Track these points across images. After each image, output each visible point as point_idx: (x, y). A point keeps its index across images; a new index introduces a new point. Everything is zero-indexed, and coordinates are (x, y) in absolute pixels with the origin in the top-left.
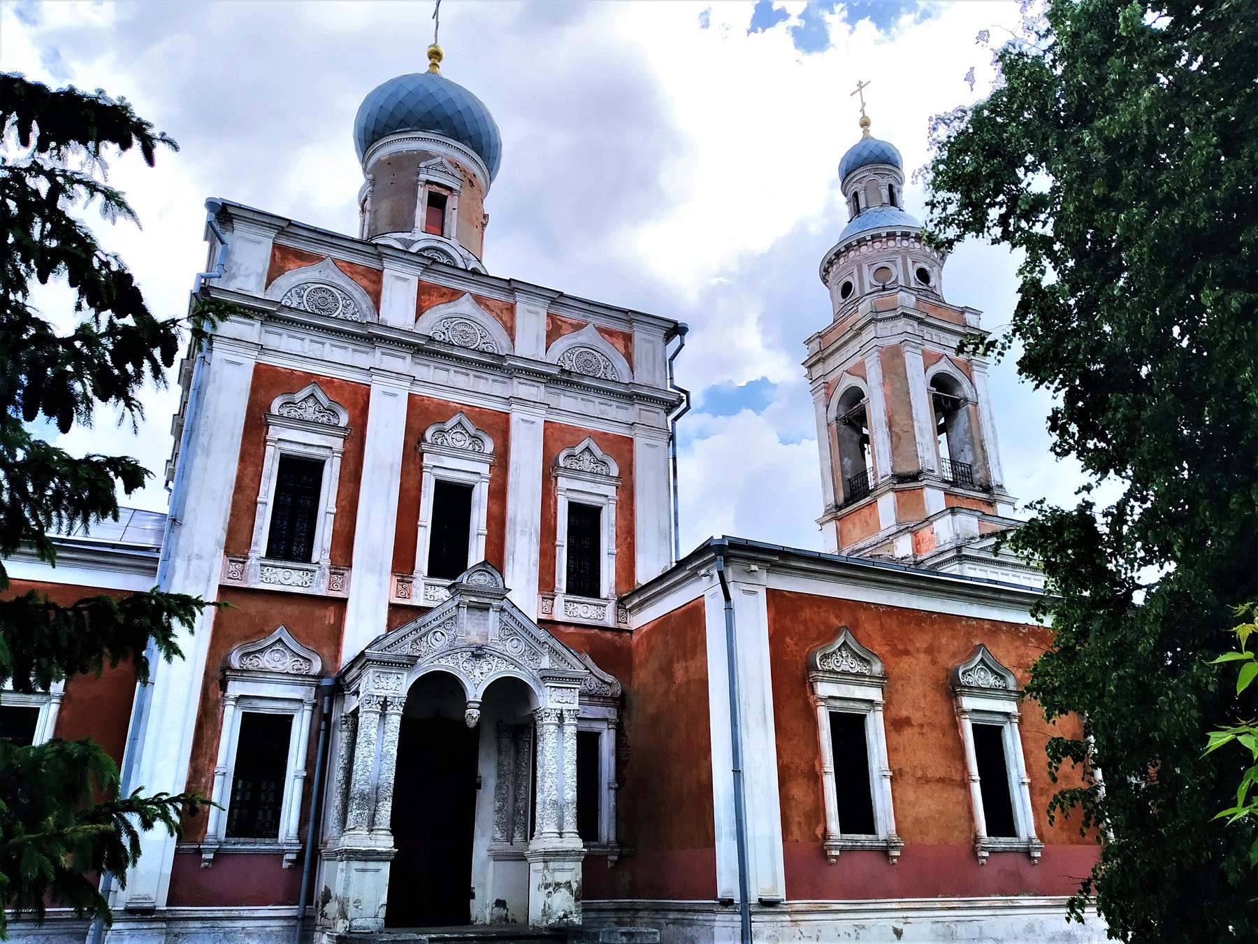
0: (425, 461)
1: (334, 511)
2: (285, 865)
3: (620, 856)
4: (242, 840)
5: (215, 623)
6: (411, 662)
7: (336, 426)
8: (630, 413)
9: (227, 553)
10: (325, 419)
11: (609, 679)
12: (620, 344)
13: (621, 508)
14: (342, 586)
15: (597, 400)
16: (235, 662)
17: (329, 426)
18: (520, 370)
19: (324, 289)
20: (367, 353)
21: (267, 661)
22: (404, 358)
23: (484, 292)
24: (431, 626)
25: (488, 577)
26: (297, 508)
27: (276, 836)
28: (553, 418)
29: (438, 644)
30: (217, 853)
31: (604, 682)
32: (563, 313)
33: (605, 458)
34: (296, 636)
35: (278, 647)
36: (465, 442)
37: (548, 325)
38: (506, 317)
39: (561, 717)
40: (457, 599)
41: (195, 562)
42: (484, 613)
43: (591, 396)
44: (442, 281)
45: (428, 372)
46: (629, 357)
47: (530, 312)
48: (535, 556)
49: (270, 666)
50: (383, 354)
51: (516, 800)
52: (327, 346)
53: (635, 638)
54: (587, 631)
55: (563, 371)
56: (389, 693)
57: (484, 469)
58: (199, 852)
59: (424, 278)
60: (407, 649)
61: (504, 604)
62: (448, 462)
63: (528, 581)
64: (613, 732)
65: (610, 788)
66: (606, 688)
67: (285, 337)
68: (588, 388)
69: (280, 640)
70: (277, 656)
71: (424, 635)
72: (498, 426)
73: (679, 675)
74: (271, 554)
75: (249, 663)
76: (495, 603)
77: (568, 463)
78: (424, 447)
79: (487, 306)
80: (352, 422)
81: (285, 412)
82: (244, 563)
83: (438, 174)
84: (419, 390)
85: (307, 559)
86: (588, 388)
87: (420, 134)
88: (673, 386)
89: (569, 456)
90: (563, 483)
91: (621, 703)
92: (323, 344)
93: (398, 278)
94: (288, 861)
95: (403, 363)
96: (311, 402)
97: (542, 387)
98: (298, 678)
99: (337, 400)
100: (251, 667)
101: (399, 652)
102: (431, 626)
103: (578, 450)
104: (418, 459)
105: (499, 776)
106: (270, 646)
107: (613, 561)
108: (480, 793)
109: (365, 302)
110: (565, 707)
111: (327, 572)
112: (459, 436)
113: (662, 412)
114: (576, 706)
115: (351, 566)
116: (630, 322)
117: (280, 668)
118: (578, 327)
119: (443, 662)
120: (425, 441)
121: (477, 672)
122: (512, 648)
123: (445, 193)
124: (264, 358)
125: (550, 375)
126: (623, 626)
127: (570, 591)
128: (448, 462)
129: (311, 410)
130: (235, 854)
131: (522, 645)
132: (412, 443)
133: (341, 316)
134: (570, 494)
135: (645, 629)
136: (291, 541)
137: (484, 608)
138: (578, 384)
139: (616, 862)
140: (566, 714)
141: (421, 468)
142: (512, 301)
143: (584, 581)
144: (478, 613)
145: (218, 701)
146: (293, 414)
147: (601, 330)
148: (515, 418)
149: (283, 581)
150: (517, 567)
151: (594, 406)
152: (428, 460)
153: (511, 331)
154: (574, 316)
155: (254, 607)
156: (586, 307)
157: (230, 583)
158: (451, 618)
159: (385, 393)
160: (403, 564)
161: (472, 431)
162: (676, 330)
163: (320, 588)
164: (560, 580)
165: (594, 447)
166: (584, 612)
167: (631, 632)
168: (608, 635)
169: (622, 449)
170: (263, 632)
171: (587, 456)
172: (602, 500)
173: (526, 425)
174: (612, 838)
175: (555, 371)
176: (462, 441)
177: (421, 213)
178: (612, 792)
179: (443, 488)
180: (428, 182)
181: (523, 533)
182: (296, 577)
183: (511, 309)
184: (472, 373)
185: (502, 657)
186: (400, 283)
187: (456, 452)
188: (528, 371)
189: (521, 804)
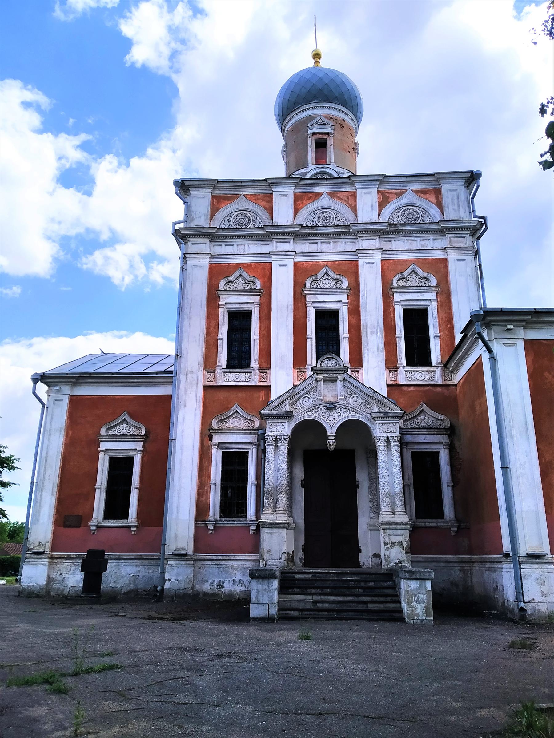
1: (258, 337)
2: (251, 532)
3: (459, 528)
4: (228, 519)
5: (203, 406)
6: (289, 416)
7: (255, 290)
8: (443, 242)
9: (205, 369)
10: (249, 287)
11: (441, 417)
12: (433, 198)
13: (442, 306)
15: (418, 239)
16: (215, 425)
17: (251, 290)
18: (361, 231)
19: (242, 213)
20: (268, 244)
21: (231, 423)
22: (289, 242)
23: (335, 189)
24: (301, 394)
25: (334, 361)
26: (240, 339)
27: (246, 517)
29: (307, 404)
30: (215, 525)
32: (389, 188)
33: (426, 275)
34: (245, 409)
35: (236, 415)
37: (379, 198)
38: (351, 201)
39: (388, 441)
41: (190, 376)
42: (335, 383)
43: (414, 236)
44: (308, 190)
45: (303, 247)
46: (439, 205)
47: (365, 193)
48: (382, 346)
49: (233, 426)
50: (277, 242)
52: (246, 246)
54: (423, 388)
55: (390, 225)
56: (278, 434)
57: (344, 298)
58: (206, 525)
59: (297, 191)
60: (288, 408)
61: (345, 376)
63: (379, 362)
64: (447, 451)
65: (448, 486)
66: (440, 423)
67: (223, 246)
68: (410, 232)
69: (236, 411)
70: (236, 420)
72: (351, 270)
75: (222, 425)
77: (400, 284)
78: (306, 292)
79: (338, 197)
80: (263, 286)
81: (227, 288)
82: (214, 372)
83: (318, 127)
84: (300, 259)
85: (248, 366)
86: (410, 232)
87: (306, 106)
88: (475, 216)
89: (400, 279)
91: (451, 431)
92: (244, 245)
93: (281, 195)
95: (289, 245)
97: (378, 239)
98: (248, 431)
99: (254, 275)
100: (223, 427)
101: (282, 410)
103: (406, 274)
104: (303, 298)
105: (370, 480)
107: (438, 341)
108: (359, 490)
109: (264, 215)
110: (390, 435)
111: (258, 371)
112: (327, 281)
113: (467, 236)
116: (438, 181)
117: (239, 427)
118: (400, 194)
119: (310, 414)
120: (305, 288)
121: (331, 418)
123: (324, 137)
124: (214, 260)
125: (382, 229)
127: (409, 364)
129: (241, 284)
130: (224, 526)
132: (299, 291)
133: (253, 226)
134: (403, 303)
135: (461, 381)
136: (238, 358)
137: (334, 380)
138: (403, 231)
139: (457, 532)
141: (306, 304)
142: (354, 189)
143: (418, 356)
145: (209, 446)
146: (232, 288)
147: (417, 192)
149: (235, 379)
151: (417, 243)
152: (309, 299)
153: (354, 209)
154: (397, 188)
155: (222, 395)
156: (404, 179)
158: (313, 388)
159: (280, 265)
161: (334, 276)
162: (472, 178)
163: (255, 381)
164: (401, 359)
165: (417, 270)
166: (420, 376)
167: (455, 385)
168: (439, 389)
169: (440, 267)
170: (228, 409)
171: (413, 276)
172: (427, 303)
173: (369, 265)
174: (452, 516)
175: (384, 227)
176: (328, 284)
177: (311, 154)
178: (450, 488)
180: (314, 134)
181: (372, 333)
182: (242, 377)
183: (354, 195)
184: (332, 241)
185: (347, 408)
186: (283, 198)
187: (325, 291)
188: (367, 231)
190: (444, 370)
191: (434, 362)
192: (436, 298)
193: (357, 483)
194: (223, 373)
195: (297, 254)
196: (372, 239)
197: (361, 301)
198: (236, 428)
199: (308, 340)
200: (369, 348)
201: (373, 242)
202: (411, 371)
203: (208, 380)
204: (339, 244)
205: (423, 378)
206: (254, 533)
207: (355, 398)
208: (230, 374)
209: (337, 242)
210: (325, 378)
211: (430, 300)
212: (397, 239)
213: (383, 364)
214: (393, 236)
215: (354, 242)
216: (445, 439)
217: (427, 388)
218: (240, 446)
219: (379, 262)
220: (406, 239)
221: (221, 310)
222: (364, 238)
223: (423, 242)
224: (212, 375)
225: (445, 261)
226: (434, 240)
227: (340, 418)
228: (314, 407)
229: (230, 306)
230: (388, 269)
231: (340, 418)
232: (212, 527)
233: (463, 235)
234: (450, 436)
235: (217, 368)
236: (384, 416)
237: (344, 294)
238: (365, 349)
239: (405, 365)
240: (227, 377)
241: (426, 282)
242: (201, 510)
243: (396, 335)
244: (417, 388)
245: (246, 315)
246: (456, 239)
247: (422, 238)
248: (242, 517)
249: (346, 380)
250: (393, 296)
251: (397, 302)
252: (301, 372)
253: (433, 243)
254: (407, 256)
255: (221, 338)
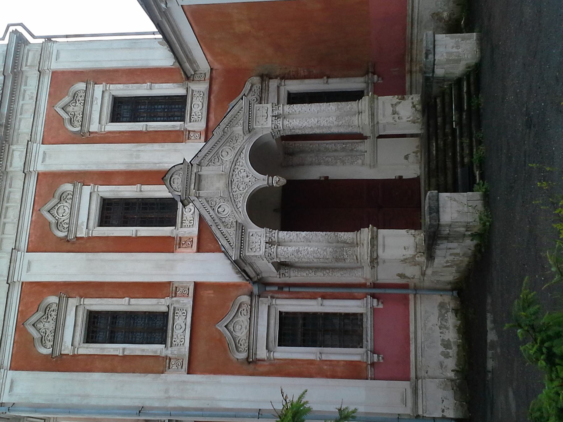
0: (83, 235)
1: (127, 299)
2: (381, 306)
3: (374, 73)
4: (364, 336)
5: (214, 374)
6: (241, 229)
7: (58, 305)
10: (54, 314)
11: (248, 86)
14: (185, 287)
15: (21, 102)
16: (242, 356)
21: (241, 333)
25: (175, 176)
27: (362, 314)
28: (39, 137)
30: (374, 352)
31: (251, 90)
33: (71, 94)
36: (65, 207)
39: (277, 117)
40: (192, 198)
41: (171, 393)
42: (203, 178)
49: (245, 331)
51: (336, 151)
53: (217, 66)
57: (87, 190)
58: (373, 364)
60: (231, 232)
62: (83, 217)
63: (175, 150)
64: (288, 82)
66: (255, 88)
71: (220, 219)
72: (50, 182)
73: (244, 27)
74: (163, 341)
76: (195, 170)
77: (78, 124)
78: (72, 237)
80: (54, 294)
81: (49, 344)
85: (165, 315)
90: (94, 127)
91: (265, 77)
94: (378, 305)
96: (40, 325)
97: (13, 147)
99: (36, 306)
100: (246, 345)
102: (214, 216)
104: (80, 241)
105: (319, 164)
106: (231, 333)
107: (157, 86)
108: (331, 177)
110: (270, 113)
111: (174, 299)
112: (61, 211)
113: (27, 47)
114: (269, 106)
115: (169, 283)
117: (246, 324)
119: (240, 205)
120: (67, 236)
121: (247, 180)
122: (228, 158)
126: (208, 76)
128: (83, 217)
129: (47, 325)
130: (374, 340)
131: (226, 148)
132: (69, 246)
134: (103, 122)
136: (153, 327)
137: (199, 178)
139: (379, 76)
140: (276, 113)
141: (89, 238)
144: (203, 183)
145: (271, 365)
146: (51, 338)
148: (41, 168)
149: (182, 330)
150: (165, 160)
152: (82, 233)
155: (202, 347)
157: (185, 366)
158: (208, 202)
159: (28, 270)
160: (166, 245)
161: (55, 201)
163: (188, 302)
164: (174, 126)
166: (197, 108)
168: (215, 88)
169: (62, 81)
171: (70, 109)
173: (47, 159)
174: (362, 79)
176: (64, 209)
178: (330, 80)
179: (104, 221)
181: (138, 157)
182: (179, 321)
185: (235, 162)
187: (74, 212)
189: (339, 147)
190: (193, 81)
191: (181, 91)
192: (102, 85)
193: (322, 179)
194: (171, 346)
195: (17, 248)
196: (12, 154)
197: (94, 168)
198: (248, 327)
199: (138, 235)
200: (156, 161)
201: (16, 154)
202: (191, 115)
203: (180, 367)
204: (12, 196)
205: (201, 103)
206: (382, 303)
207: (223, 153)
208: (175, 336)
209: (8, 199)
210: (196, 188)
211: (103, 92)
212: (17, 127)
213: (179, 146)
214: (12, 131)
215: (11, 178)
216: (273, 84)
217: (213, 100)
218: (272, 322)
219: (44, 147)
220: (19, 116)
221: (82, 351)
222: (8, 164)
223: (27, 97)
224: (173, 362)
225: (55, 74)
226: (26, 85)
227: (247, 169)
228: (232, 200)
229: (77, 339)
230: (56, 134)
231: (247, 169)
232: (376, 356)
233: (26, 51)
234: (271, 78)
235: (163, 355)
236: (248, 118)
237: (81, 189)
238: (158, 165)
239: (182, 123)
240: (178, 341)
241: (79, 95)
242: (353, 372)
243: (144, 130)
244: (212, 110)
245: (93, 318)
246: (29, 60)
247: (21, 98)
248: (362, 320)
249: (200, 162)
250: (92, 133)
251: (101, 128)
252: (180, 244)
253: (30, 85)
254: (42, 116)
255: (121, 351)
